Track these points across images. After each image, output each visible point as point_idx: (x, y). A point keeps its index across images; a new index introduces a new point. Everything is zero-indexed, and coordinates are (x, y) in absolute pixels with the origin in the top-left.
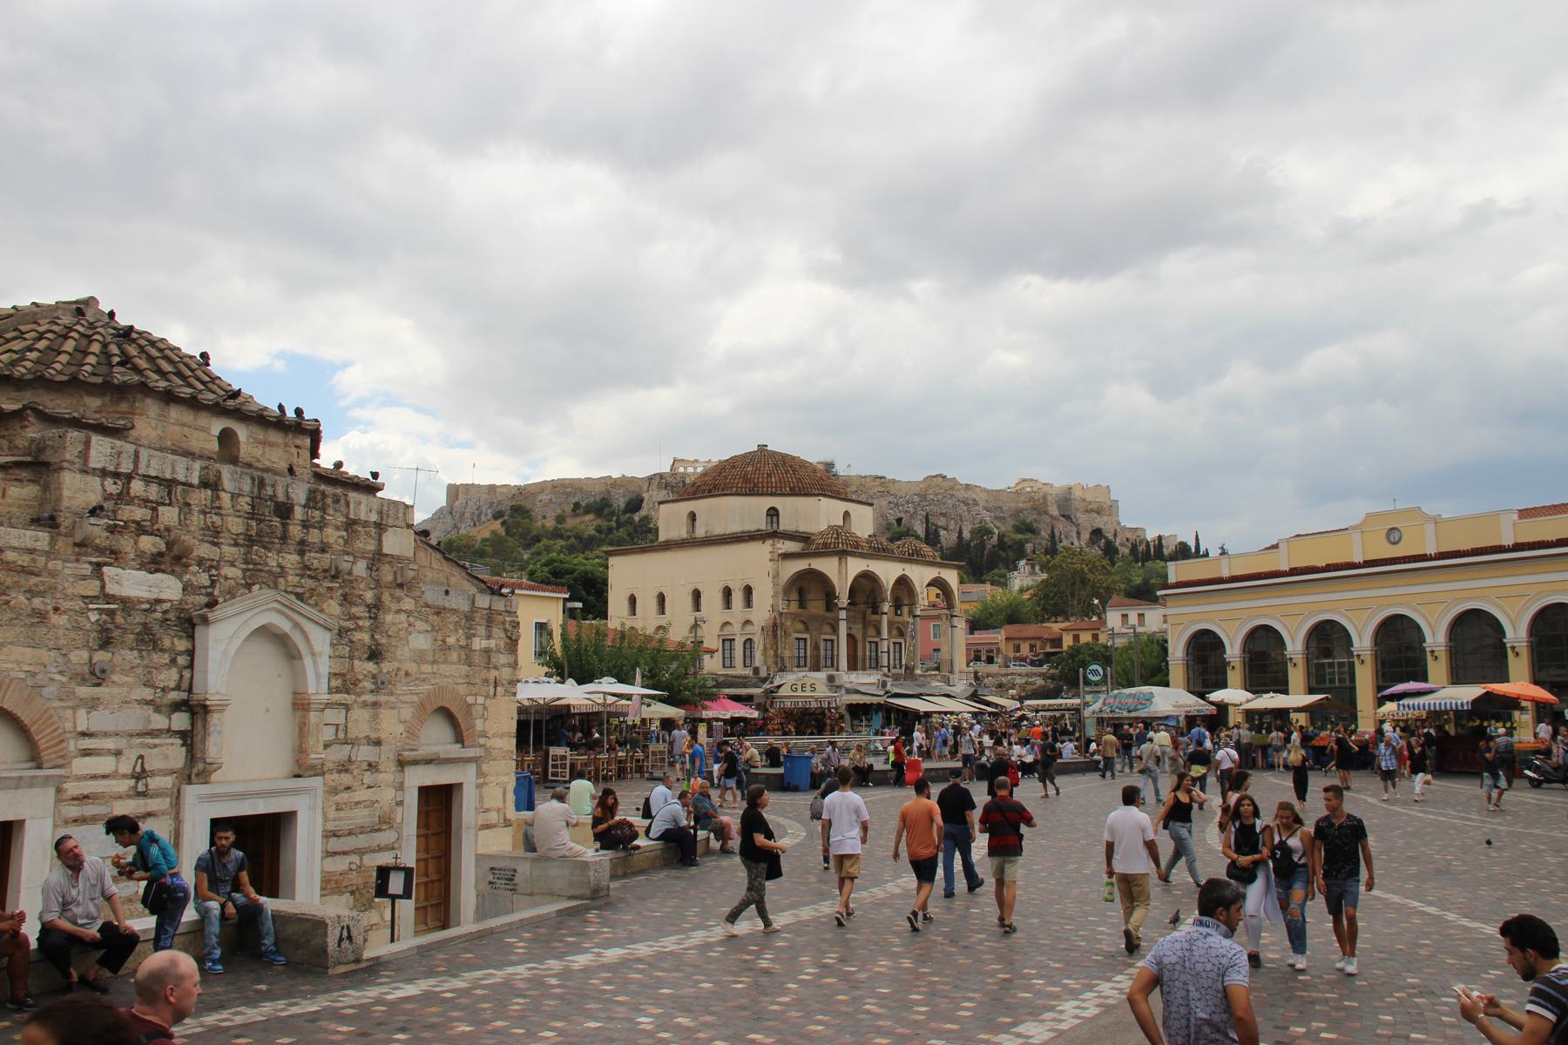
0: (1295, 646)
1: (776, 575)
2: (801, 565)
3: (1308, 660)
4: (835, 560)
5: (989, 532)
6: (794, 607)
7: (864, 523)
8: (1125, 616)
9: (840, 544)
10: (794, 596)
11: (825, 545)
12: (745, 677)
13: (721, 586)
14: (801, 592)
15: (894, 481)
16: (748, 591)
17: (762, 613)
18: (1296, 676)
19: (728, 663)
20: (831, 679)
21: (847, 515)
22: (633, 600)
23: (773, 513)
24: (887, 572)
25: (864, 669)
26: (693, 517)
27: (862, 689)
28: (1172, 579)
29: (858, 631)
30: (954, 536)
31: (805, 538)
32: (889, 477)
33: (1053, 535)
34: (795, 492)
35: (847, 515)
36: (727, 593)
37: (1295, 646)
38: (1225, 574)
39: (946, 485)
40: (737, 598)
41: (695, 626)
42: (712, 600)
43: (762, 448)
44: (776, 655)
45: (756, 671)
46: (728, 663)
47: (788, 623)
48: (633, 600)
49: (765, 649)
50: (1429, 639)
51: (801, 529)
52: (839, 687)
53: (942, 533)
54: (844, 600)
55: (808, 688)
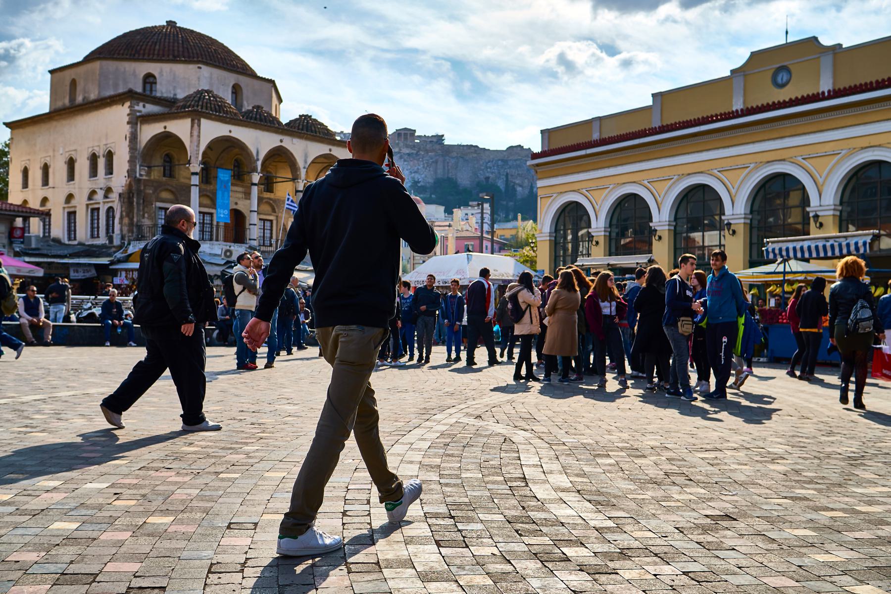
0: (661, 218)
1: (133, 138)
3: (676, 234)
4: (188, 121)
6: (157, 174)
9: (201, 106)
10: (158, 161)
11: (184, 107)
16: (110, 156)
17: (119, 181)
22: (25, 172)
23: (149, 79)
24: (259, 142)
25: (217, 240)
29: (242, 206)
30: (527, 191)
32: (481, 146)
34: (175, 59)
36: (94, 158)
37: (661, 218)
38: (596, 136)
40: (101, 162)
41: (70, 197)
42: (82, 166)
43: (171, 24)
44: (131, 224)
48: (25, 172)
49: (121, 218)
50: (814, 201)
53: (519, 189)
54: (196, 167)
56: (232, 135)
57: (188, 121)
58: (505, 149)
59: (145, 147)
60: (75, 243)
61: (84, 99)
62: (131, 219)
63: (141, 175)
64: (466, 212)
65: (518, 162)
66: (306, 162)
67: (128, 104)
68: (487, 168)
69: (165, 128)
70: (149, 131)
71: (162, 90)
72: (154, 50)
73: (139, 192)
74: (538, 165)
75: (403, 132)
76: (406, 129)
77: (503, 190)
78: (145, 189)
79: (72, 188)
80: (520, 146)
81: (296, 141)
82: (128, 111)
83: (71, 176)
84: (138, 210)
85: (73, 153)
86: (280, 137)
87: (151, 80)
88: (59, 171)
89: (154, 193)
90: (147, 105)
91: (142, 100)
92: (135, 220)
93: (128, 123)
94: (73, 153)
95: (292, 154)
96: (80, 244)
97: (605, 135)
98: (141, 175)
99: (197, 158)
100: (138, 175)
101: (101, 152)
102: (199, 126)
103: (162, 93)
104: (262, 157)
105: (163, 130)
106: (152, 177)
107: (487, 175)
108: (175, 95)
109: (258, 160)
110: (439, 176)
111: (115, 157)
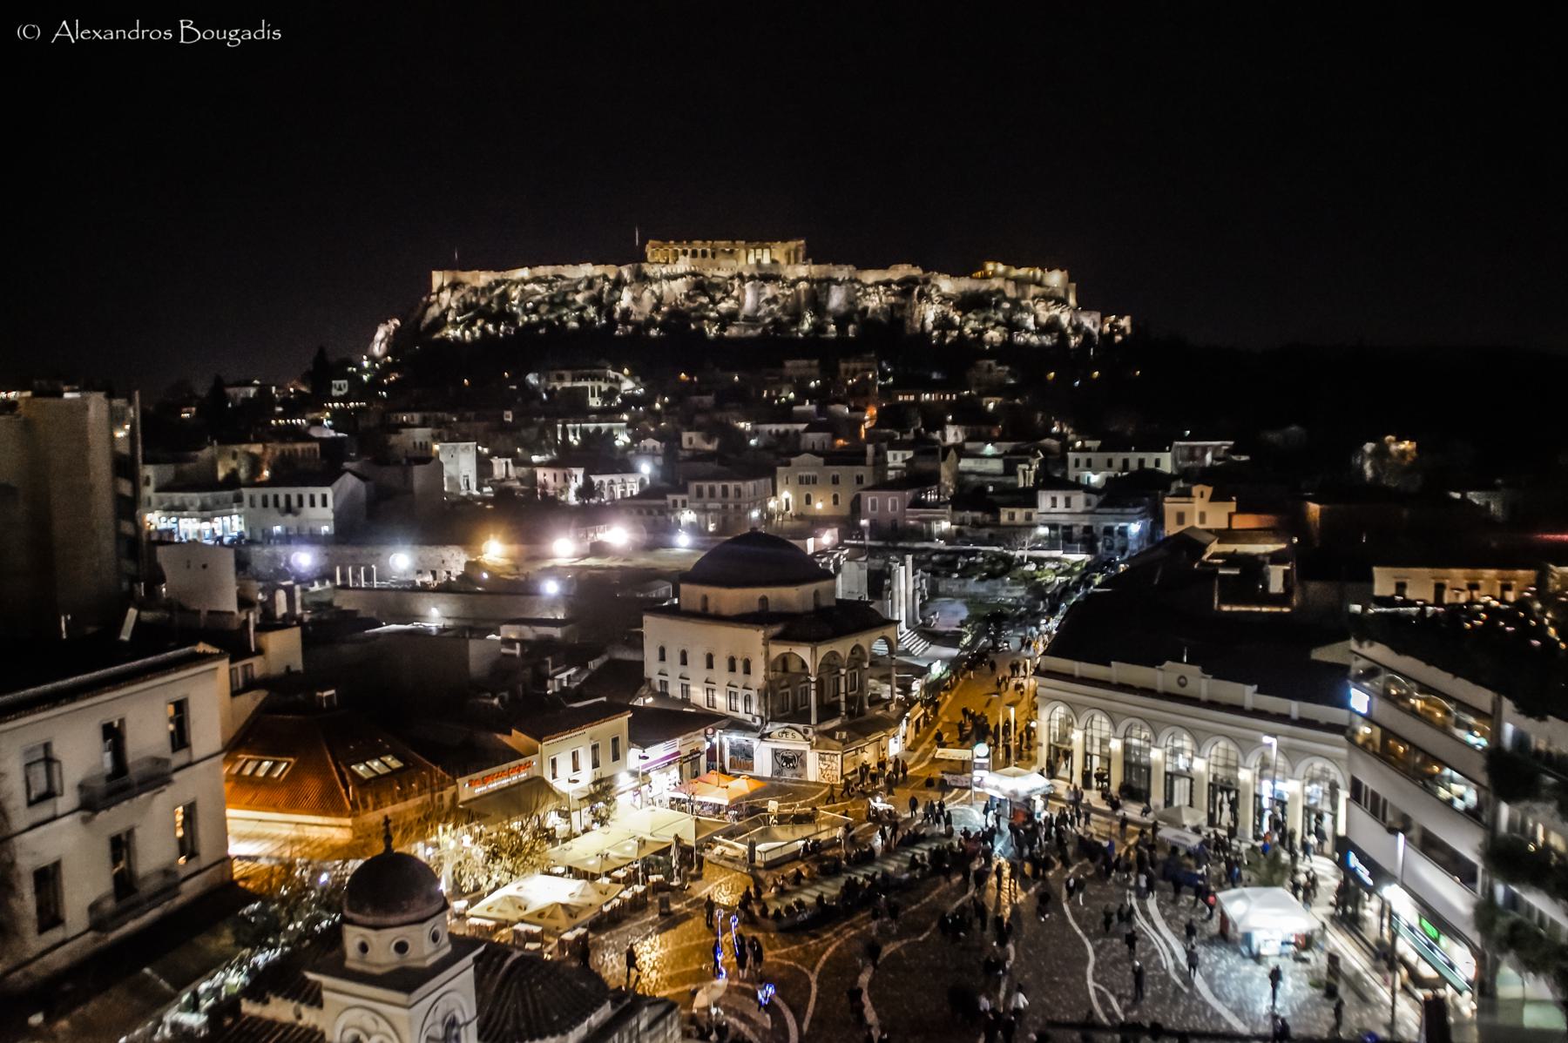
1: (767, 654)
8: (1054, 500)
22: (662, 650)
40: (739, 665)
42: (721, 662)
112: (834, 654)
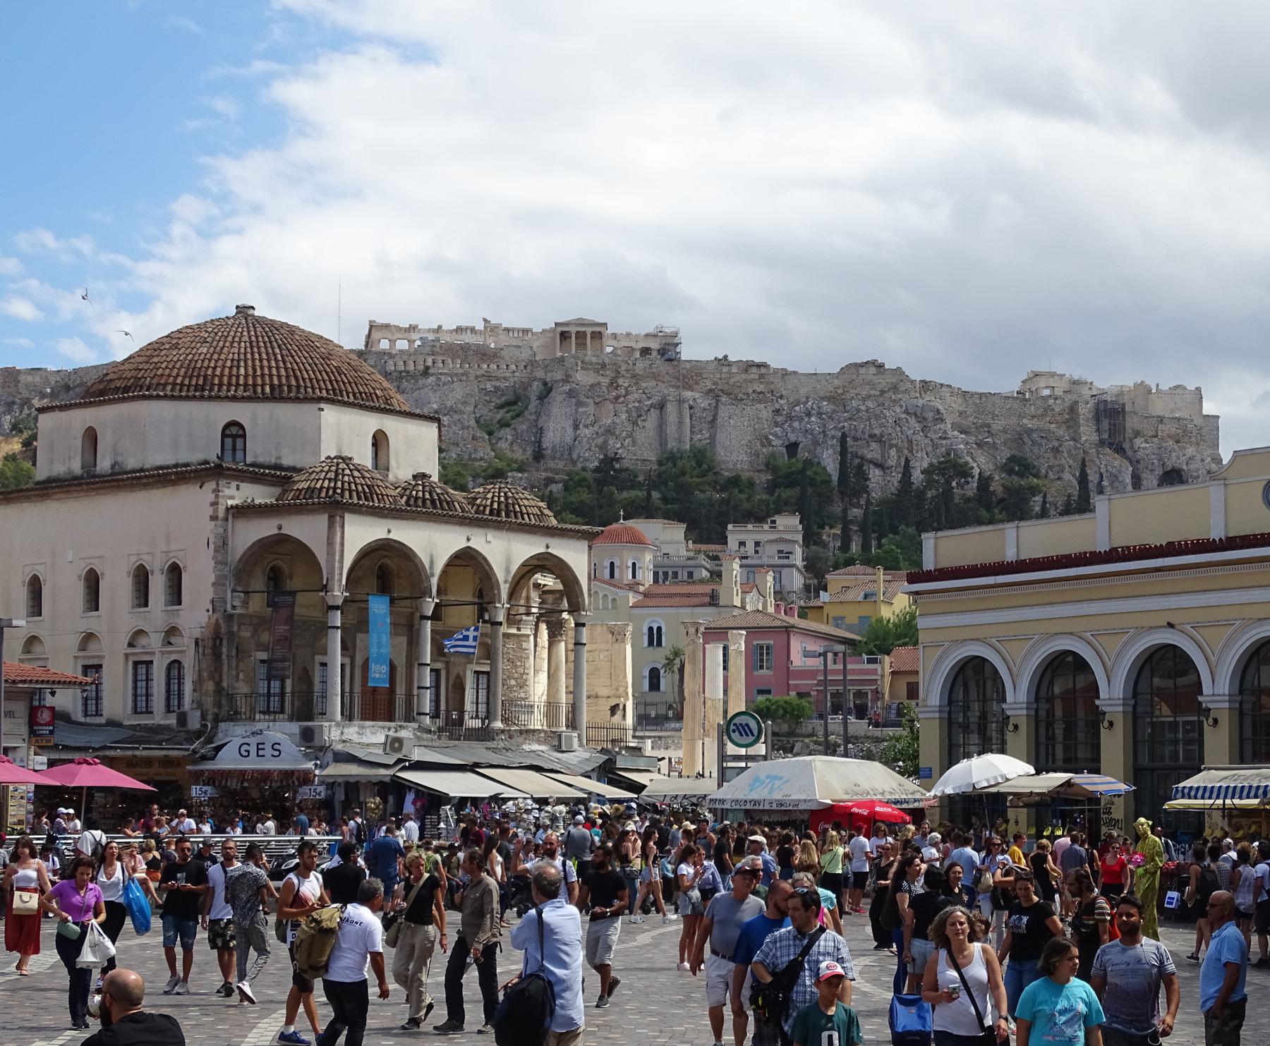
1: (223, 544)
2: (265, 528)
4: (323, 519)
5: (963, 472)
6: (257, 604)
7: (416, 450)
10: (259, 582)
12: (167, 728)
13: (133, 562)
14: (275, 577)
15: (785, 373)
16: (175, 573)
17: (196, 615)
18: (1113, 744)
19: (142, 704)
20: (307, 736)
21: (379, 441)
23: (234, 433)
24: (433, 544)
26: (91, 436)
27: (360, 754)
28: (929, 564)
30: (896, 478)
31: (278, 475)
32: (774, 364)
33: (1083, 480)
34: (276, 396)
35: (379, 441)
36: (141, 578)
39: (884, 382)
40: (158, 586)
41: (89, 637)
42: (117, 588)
43: (243, 310)
44: (219, 691)
45: (182, 719)
46: (142, 704)
47: (246, 634)
49: (198, 684)
51: (286, 462)
52: (323, 749)
53: (875, 474)
54: (338, 594)
55: (268, 751)
56: (391, 536)
57: (323, 519)
58: (837, 370)
59: (241, 559)
60: (102, 720)
61: (113, 467)
62: (218, 684)
63: (234, 607)
64: (743, 537)
65: (870, 404)
66: (508, 571)
67: (210, 486)
68: (790, 418)
69: (280, 528)
70: (250, 533)
71: (257, 450)
72: (238, 376)
73: (231, 634)
74: (917, 593)
75: (573, 330)
76: (581, 323)
77: (835, 478)
78: (239, 630)
79: (93, 623)
80: (873, 363)
81: (491, 535)
82: (212, 498)
83: (93, 600)
84: (229, 668)
85: (95, 561)
86: (467, 531)
87: (234, 430)
88: (65, 592)
89: (253, 636)
90: (242, 485)
91: (236, 478)
92: (225, 684)
93: (214, 518)
94: (95, 561)
95: (485, 559)
96: (112, 723)
97: (1028, 554)
98: (234, 607)
99: (340, 580)
100: (229, 607)
101: (157, 566)
102: (343, 527)
103: (256, 455)
104: (438, 569)
105: (276, 531)
106: (251, 610)
107: (793, 438)
108: (279, 458)
109: (433, 575)
110: (672, 444)
111: (185, 577)
112: (402, 553)
